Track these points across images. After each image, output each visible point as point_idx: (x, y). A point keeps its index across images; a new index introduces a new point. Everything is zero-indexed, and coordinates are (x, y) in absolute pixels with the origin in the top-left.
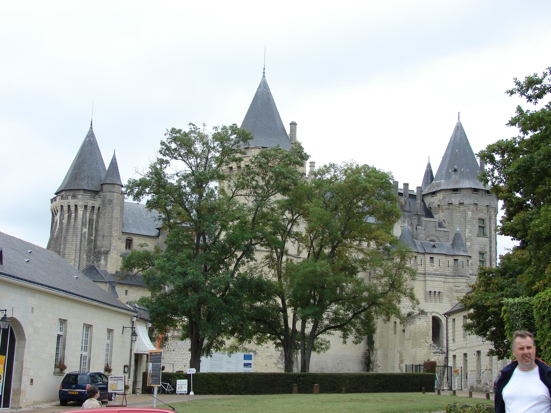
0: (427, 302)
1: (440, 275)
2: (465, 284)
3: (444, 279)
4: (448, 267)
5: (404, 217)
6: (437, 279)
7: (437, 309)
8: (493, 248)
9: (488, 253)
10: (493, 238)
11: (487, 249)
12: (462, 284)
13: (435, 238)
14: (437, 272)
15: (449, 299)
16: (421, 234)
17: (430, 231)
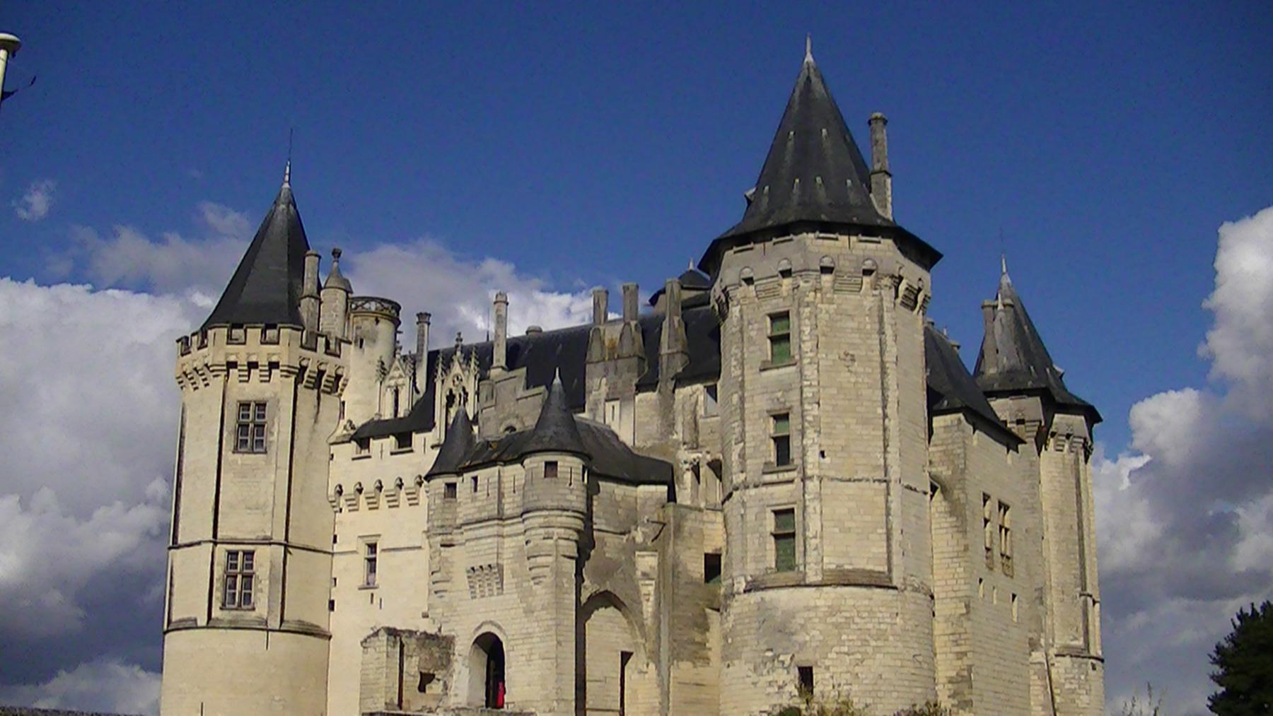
0: (475, 597)
1: (489, 520)
2: (542, 531)
3: (496, 528)
4: (514, 492)
5: (615, 374)
6: (482, 532)
7: (492, 614)
8: (805, 390)
9: (797, 409)
10: (806, 361)
11: (795, 396)
12: (533, 532)
13: (513, 422)
14: (484, 515)
15: (515, 580)
16: (488, 419)
17: (506, 406)
